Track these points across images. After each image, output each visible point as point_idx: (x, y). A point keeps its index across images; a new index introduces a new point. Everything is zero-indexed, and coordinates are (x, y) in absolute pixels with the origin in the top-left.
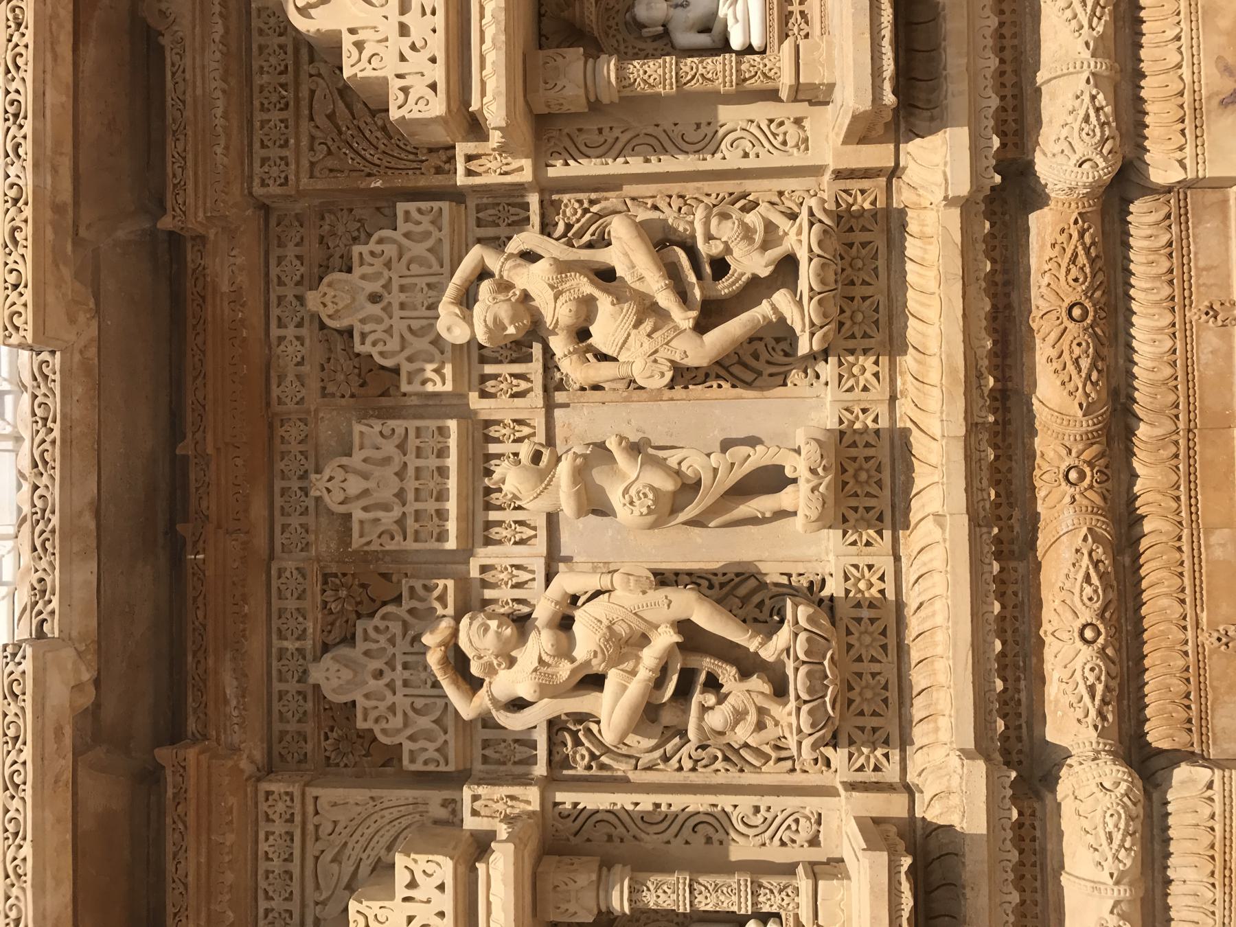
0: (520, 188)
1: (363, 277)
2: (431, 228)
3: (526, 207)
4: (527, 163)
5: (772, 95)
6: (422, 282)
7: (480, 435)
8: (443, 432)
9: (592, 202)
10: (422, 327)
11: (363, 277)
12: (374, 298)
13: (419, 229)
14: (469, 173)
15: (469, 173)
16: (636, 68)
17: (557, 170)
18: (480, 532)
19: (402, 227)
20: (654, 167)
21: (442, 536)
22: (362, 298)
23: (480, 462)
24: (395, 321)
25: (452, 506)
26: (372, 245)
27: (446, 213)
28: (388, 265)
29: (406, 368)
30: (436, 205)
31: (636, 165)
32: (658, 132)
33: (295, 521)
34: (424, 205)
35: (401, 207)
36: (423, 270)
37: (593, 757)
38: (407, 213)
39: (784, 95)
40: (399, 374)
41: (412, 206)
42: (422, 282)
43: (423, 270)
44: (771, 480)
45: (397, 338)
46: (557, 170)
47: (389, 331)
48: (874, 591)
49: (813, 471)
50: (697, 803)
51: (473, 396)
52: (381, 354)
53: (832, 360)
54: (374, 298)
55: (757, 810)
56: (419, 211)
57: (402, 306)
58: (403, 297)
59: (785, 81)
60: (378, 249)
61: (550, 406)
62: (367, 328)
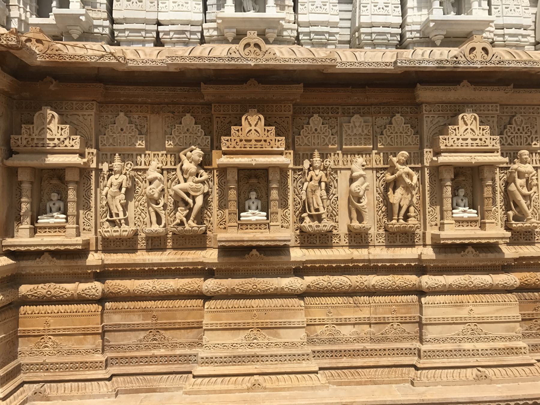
0: (422, 162)
1: (403, 127)
3: (418, 164)
4: (428, 165)
5: (442, 218)
7: (368, 153)
8: (370, 144)
14: (427, 152)
15: (427, 152)
16: (449, 189)
17: (427, 171)
18: (346, 153)
19: (414, 136)
20: (427, 193)
21: (346, 145)
23: (360, 153)
24: (394, 134)
25: (353, 147)
28: (406, 133)
31: (427, 188)
32: (434, 194)
37: (296, 179)
39: (442, 221)
41: (418, 138)
44: (360, 219)
46: (427, 171)
48: (334, 241)
49: (364, 227)
50: (290, 202)
51: (376, 151)
53: (384, 232)
55: (289, 214)
57: (397, 136)
59: (446, 222)
61: (372, 169)
62: (392, 128)
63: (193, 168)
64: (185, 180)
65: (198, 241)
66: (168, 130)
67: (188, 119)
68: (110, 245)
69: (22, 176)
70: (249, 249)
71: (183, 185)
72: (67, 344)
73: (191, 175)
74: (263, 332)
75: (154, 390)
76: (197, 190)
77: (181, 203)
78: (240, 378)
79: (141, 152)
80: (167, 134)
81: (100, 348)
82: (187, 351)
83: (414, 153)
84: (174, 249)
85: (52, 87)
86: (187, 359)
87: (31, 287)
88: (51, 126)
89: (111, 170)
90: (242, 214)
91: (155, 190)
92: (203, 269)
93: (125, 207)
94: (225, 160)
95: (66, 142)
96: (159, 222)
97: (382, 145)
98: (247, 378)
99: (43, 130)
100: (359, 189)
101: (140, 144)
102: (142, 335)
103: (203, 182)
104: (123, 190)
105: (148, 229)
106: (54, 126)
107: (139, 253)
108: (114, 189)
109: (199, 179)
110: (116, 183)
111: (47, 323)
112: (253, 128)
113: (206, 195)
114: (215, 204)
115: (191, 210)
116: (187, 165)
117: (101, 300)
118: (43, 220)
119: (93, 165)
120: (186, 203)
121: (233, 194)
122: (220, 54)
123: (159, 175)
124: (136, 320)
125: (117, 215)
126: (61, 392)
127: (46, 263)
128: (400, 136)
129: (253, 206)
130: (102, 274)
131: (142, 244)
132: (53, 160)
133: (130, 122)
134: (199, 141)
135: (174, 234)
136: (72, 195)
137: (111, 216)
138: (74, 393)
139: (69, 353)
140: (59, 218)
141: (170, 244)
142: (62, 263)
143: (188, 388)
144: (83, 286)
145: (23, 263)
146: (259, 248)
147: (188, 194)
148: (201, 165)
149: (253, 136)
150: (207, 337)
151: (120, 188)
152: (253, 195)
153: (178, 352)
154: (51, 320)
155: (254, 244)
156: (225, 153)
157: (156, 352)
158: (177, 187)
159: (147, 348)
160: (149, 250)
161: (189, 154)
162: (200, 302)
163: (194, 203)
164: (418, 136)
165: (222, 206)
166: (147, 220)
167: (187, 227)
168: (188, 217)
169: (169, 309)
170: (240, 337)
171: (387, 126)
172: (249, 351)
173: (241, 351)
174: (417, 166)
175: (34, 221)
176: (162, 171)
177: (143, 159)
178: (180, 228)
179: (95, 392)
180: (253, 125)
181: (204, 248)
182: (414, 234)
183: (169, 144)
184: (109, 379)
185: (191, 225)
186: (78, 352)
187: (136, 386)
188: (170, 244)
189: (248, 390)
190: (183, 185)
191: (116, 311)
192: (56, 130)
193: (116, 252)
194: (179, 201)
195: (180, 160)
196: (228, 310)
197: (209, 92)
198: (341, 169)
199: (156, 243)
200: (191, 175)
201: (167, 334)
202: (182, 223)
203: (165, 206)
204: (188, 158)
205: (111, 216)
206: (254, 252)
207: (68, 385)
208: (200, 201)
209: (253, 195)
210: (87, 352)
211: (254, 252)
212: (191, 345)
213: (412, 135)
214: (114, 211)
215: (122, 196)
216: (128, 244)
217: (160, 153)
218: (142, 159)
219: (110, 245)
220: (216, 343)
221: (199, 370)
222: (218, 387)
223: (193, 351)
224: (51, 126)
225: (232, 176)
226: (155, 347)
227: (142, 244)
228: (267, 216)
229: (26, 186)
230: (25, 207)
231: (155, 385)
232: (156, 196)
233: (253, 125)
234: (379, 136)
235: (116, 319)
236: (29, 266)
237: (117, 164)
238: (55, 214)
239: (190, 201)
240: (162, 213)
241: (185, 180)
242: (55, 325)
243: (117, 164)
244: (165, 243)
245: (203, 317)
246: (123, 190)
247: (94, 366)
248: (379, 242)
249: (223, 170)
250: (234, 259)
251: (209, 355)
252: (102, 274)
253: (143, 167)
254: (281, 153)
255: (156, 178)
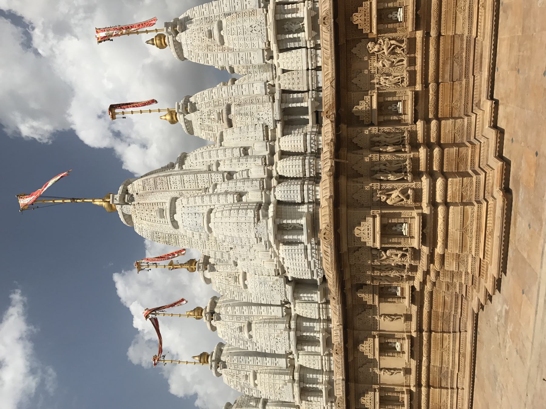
63: (377, 46)
64: (383, 49)
65: (412, 42)
66: (359, 60)
67: (354, 51)
68: (412, 83)
69: (382, 119)
70: (416, 14)
71: (385, 51)
72: (457, 95)
73: (380, 47)
74: (458, 4)
75: (482, 55)
76: (388, 43)
77: (394, 51)
78: (480, 14)
79: (370, 72)
80: (361, 59)
81: (460, 82)
82: (465, 42)
84: (415, 53)
85: (343, 110)
86: (468, 41)
87: (430, 114)
88: (360, 109)
89: (377, 84)
90: (399, 20)
91: (387, 63)
92: (426, 38)
93: (395, 77)
94: (374, 31)
95: (367, 102)
96: (402, 60)
98: (480, 10)
99: (362, 111)
101: (366, 72)
102: (455, 64)
103: (384, 41)
104: (387, 77)
105: (405, 65)
106: (360, 108)
107: (416, 69)
108: (387, 81)
109: (382, 43)
110: (384, 81)
111: (446, 106)
112: (359, 18)
113: (390, 39)
114: (394, 35)
115: (397, 46)
116: (376, 49)
117: (438, 84)
118: (401, 111)
119: (376, 91)
120: (394, 48)
121: (391, 26)
122: (326, 36)
123: (381, 62)
124: (448, 68)
125: (399, 79)
126: (478, 96)
127: (420, 108)
129: (396, 15)
130: (426, 84)
131: (412, 68)
132: (375, 106)
133: (356, 77)
134: (364, 45)
135: (408, 54)
136: (390, 99)
137: (399, 82)
138: (478, 90)
139: (461, 95)
140: (400, 104)
141: (413, 55)
142: (420, 101)
143: (482, 38)
144: (431, 92)
145: (420, 117)
146: (417, 10)
147: (389, 48)
148: (376, 43)
149: (363, 18)
150: (458, 32)
151: (387, 79)
152: (390, 16)
153: (465, 46)
154: (446, 104)
155: (415, 13)
156: (371, 32)
157: (464, 56)
158: (386, 53)
159: (462, 61)
160: (415, 64)
161: (370, 49)
162: (441, 38)
163: (393, 44)
165: (395, 31)
166: (400, 67)
167: (405, 47)
168: (400, 47)
169: (444, 53)
170: (460, 16)
172: (467, 11)
173: (467, 15)
175: (401, 114)
176: (378, 61)
177: (373, 70)
178: (405, 50)
179: (479, 80)
180: (358, 19)
181: (415, 38)
183: (366, 59)
184: (474, 76)
185: (404, 45)
186: (461, 91)
187: (479, 64)
188: (413, 55)
189: (485, 9)
190: (385, 51)
191: (443, 77)
192: (362, 106)
193: (416, 79)
194: (393, 52)
195: (373, 53)
196: (446, 23)
197: (342, 41)
199: (412, 62)
200: (380, 47)
201: (456, 52)
202: (403, 50)
203: (395, 59)
204: (373, 49)
205: (399, 82)
206: (418, 12)
207: (475, 93)
208: (393, 42)
209: (390, 16)
210: (461, 87)
211: (418, 12)
212: (462, 40)
214: (397, 81)
215: (390, 78)
216: (412, 74)
217: (370, 63)
218: (373, 71)
219: (412, 83)
220: (462, 28)
221: (474, 34)
222: (482, 24)
223: (465, 39)
224: (360, 109)
225: (381, 26)
226: (462, 57)
227: (412, 68)
228: (401, 8)
229: (386, 118)
230: (395, 118)
231: (479, 55)
232: (390, 62)
233: (358, 19)
235: (447, 76)
236: (421, 114)
237: (375, 81)
238: (398, 106)
239: (393, 46)
240: (398, 59)
241: (383, 49)
242: (447, 103)
243: (375, 81)
244: (412, 57)
245: (449, 36)
246: (387, 77)
247: (467, 83)
249: (379, 31)
250: (422, 23)
251: (467, 30)
252: (426, 84)
253: (376, 70)
254: (371, 3)
255: (382, 63)
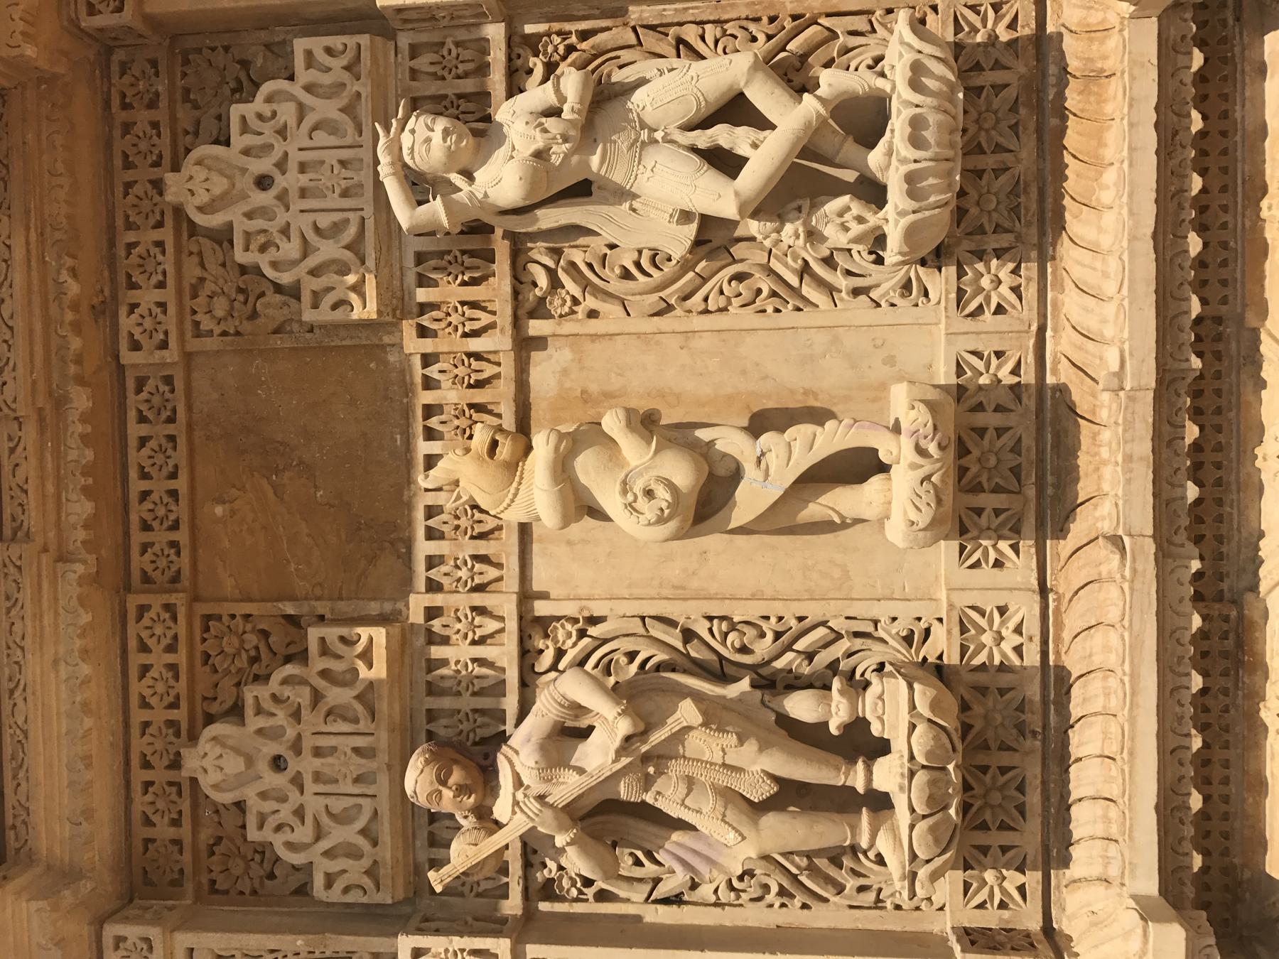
1: (246, 152)
2: (346, 77)
6: (331, 157)
9: (584, 35)
10: (335, 224)
11: (246, 152)
12: (263, 182)
13: (326, 79)
19: (303, 76)
22: (246, 183)
26: (259, 104)
27: (366, 55)
29: (311, 285)
30: (351, 41)
33: (161, 537)
34: (336, 41)
35: (300, 45)
36: (333, 141)
38: (309, 54)
40: (299, 299)
41: (317, 44)
42: (331, 157)
43: (333, 141)
45: (296, 242)
47: (285, 231)
52: (275, 265)
54: (263, 182)
56: (329, 51)
57: (303, 193)
58: (304, 180)
60: (267, 110)
61: (525, 345)
83: (414, 74)
97: (358, 288)
100: (649, 493)
128: (303, 168)
164: (300, 45)
171: (240, 256)
174: (497, 56)
182: (958, 48)
198: (526, 596)
213: (296, 89)
234: (309, 315)
248: (1016, 290)
